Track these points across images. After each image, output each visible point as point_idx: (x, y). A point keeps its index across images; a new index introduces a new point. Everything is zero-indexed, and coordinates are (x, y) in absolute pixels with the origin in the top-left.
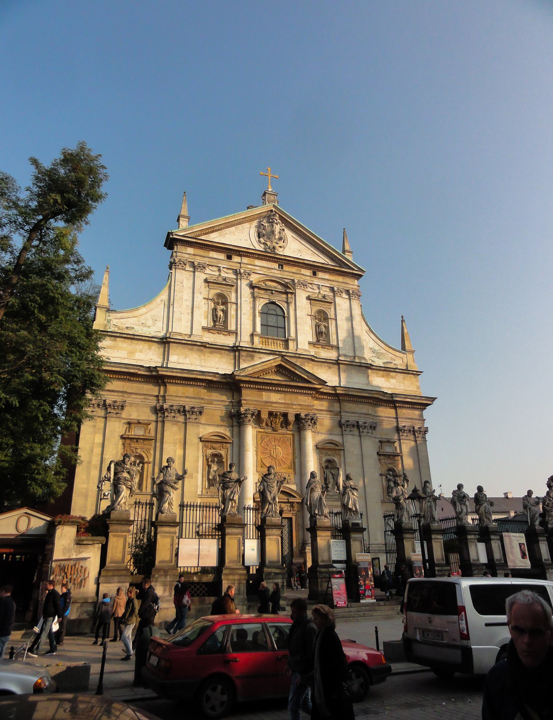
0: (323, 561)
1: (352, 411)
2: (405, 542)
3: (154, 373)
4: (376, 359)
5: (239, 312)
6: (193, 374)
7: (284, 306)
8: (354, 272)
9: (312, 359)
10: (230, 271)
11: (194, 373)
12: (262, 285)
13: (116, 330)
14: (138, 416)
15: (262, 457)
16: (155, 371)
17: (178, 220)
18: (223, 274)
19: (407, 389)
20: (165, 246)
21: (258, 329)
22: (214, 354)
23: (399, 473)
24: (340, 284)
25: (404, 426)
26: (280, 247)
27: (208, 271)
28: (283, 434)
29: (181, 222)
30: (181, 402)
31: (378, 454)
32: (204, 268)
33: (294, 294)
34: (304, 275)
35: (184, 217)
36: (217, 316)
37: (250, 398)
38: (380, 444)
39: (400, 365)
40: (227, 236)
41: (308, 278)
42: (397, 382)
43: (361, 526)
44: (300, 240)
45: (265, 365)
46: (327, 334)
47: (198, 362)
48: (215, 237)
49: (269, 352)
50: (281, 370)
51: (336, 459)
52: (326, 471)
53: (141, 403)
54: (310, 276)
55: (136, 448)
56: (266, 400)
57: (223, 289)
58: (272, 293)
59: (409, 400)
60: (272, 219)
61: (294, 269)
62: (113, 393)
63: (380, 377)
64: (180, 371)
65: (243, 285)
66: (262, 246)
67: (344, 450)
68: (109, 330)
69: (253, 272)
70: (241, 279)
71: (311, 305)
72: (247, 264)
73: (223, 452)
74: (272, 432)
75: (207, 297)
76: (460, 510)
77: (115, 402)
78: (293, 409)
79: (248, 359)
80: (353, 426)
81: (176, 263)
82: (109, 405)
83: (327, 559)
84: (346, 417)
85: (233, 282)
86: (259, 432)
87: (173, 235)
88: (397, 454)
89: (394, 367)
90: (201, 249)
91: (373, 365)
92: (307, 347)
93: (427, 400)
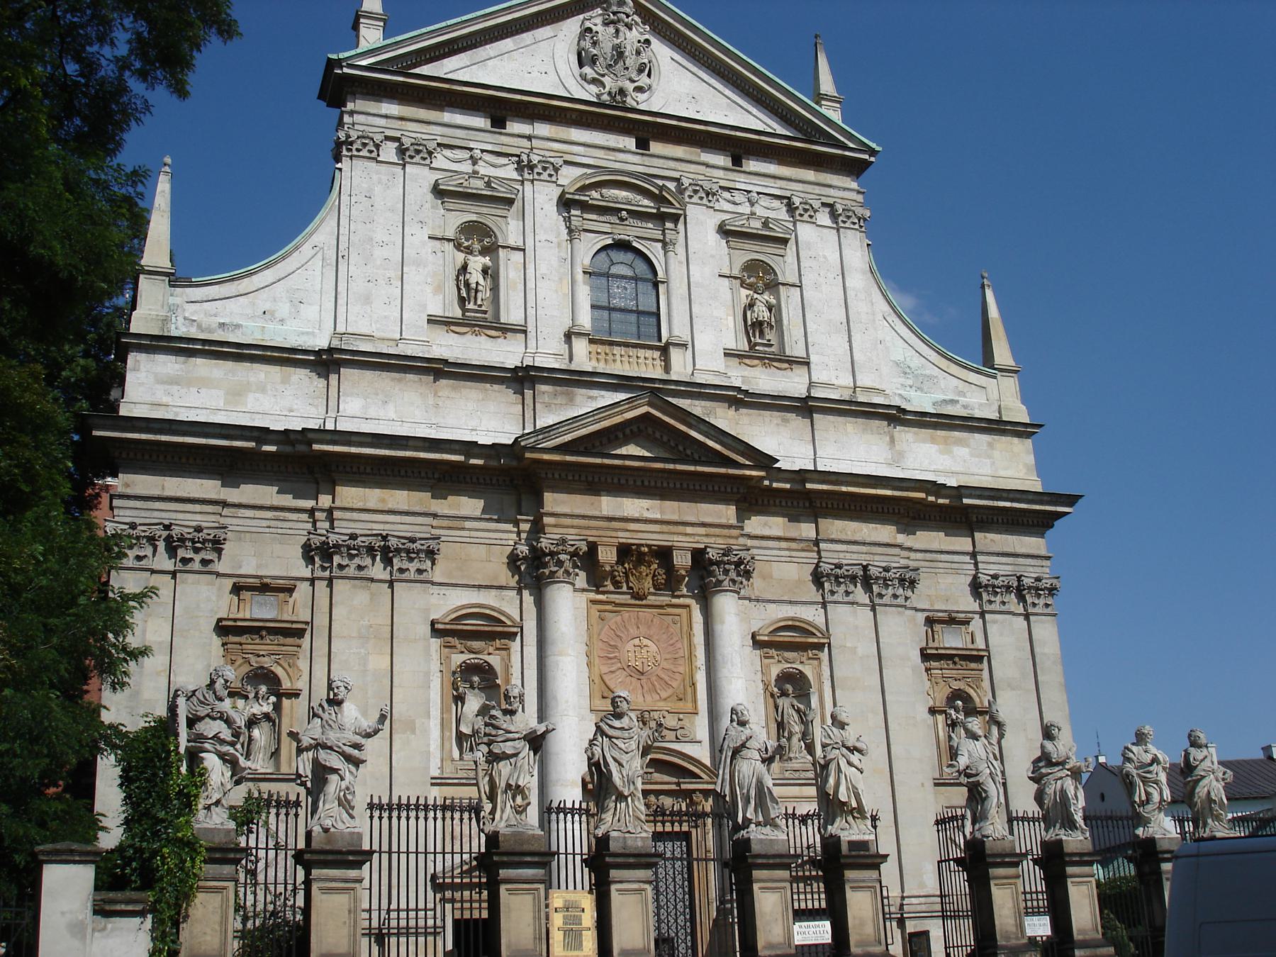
0: (770, 946)
1: (850, 538)
2: (994, 889)
3: (301, 448)
4: (912, 394)
6: (406, 448)
7: (655, 251)
8: (847, 153)
9: (740, 399)
11: (411, 443)
13: (193, 332)
14: (259, 566)
15: (605, 669)
16: (301, 442)
17: (356, 27)
18: (483, 169)
19: (1002, 473)
20: (320, 97)
21: (585, 320)
22: (465, 392)
23: (981, 702)
24: (809, 188)
25: (995, 577)
26: (639, 89)
27: (440, 161)
28: (661, 607)
29: (363, 31)
30: (375, 526)
31: (925, 656)
34: (707, 165)
35: (371, 16)
36: (467, 285)
39: (981, 405)
40: (490, 63)
41: (721, 173)
42: (972, 455)
43: (873, 850)
44: (695, 69)
47: (419, 415)
48: (456, 68)
50: (650, 430)
52: (780, 702)
54: (725, 169)
55: (259, 656)
56: (611, 514)
57: (485, 210)
58: (622, 219)
60: (614, 13)
61: (679, 151)
62: (189, 507)
63: (924, 441)
64: (369, 440)
66: (594, 89)
67: (829, 644)
68: (174, 333)
69: (566, 162)
70: (532, 181)
73: (495, 660)
74: (633, 602)
76: (1144, 798)
77: (199, 529)
78: (686, 534)
79: (559, 400)
80: (853, 578)
81: (351, 143)
82: (179, 540)
83: (781, 940)
84: (833, 554)
86: (594, 602)
87: (341, 67)
89: (963, 413)
91: (904, 411)
92: (719, 363)
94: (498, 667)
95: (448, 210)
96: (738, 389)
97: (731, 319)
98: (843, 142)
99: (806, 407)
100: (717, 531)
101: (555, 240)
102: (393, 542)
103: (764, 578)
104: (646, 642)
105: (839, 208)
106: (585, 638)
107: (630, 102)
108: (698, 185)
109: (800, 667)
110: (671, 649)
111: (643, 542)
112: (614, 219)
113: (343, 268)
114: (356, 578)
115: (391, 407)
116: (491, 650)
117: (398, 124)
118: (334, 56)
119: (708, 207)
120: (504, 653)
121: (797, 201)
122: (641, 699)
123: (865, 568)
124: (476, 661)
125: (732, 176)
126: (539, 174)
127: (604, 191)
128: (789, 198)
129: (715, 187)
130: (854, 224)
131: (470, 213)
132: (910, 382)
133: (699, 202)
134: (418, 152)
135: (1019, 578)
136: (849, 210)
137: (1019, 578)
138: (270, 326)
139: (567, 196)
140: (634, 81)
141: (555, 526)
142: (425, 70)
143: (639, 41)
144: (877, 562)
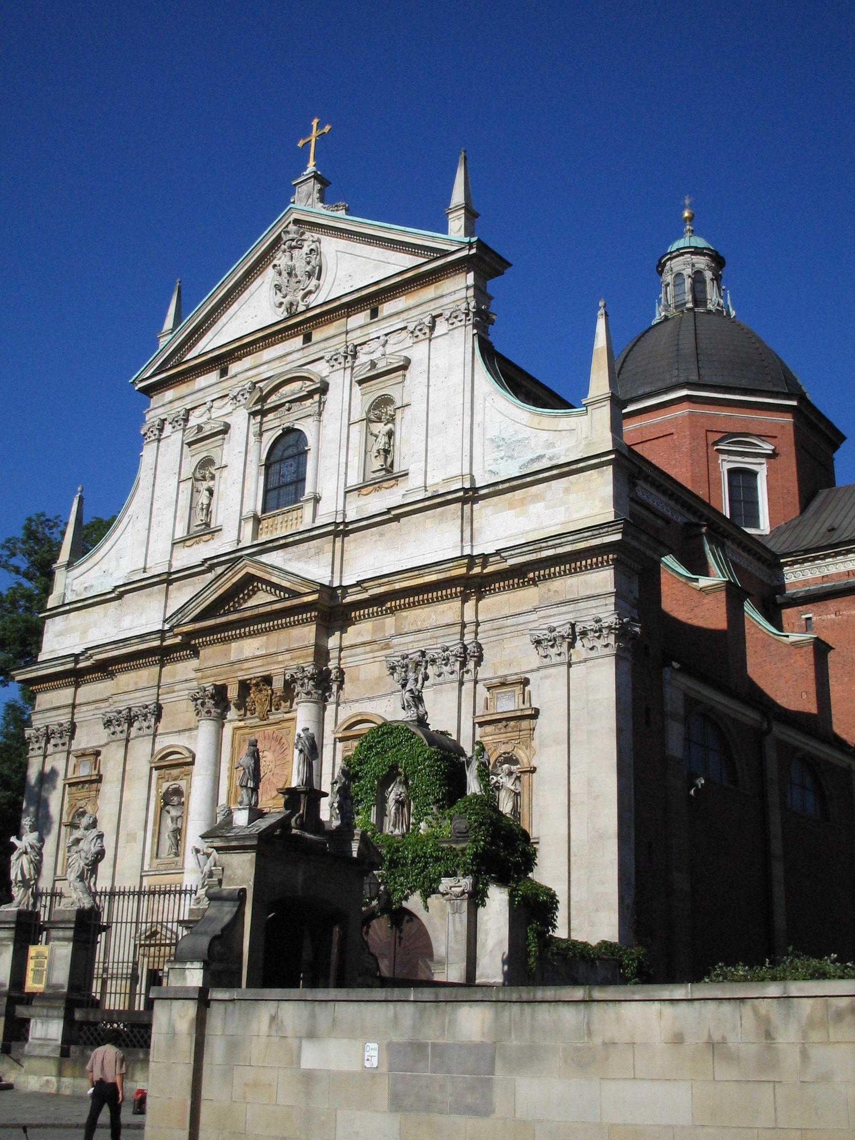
7: (307, 427)
11: (132, 641)
12: (273, 400)
19: (575, 516)
24: (424, 308)
25: (552, 630)
26: (310, 292)
27: (193, 421)
32: (186, 420)
33: (323, 389)
37: (210, 664)
38: (487, 695)
39: (568, 450)
41: (358, 333)
45: (219, 588)
53: (93, 717)
57: (210, 446)
59: (551, 552)
65: (240, 420)
71: (363, 395)
72: (246, 371)
73: (183, 784)
78: (279, 662)
86: (237, 729)
88: (519, 713)
90: (184, 383)
93: (599, 536)
95: (193, 456)
96: (337, 524)
97: (357, 458)
98: (447, 251)
99: (393, 516)
100: (298, 653)
101: (244, 450)
103: (352, 681)
107: (301, 308)
108: (337, 354)
110: (281, 756)
111: (252, 676)
114: (119, 740)
115: (144, 616)
117: (168, 407)
118: (131, 381)
119: (345, 369)
120: (189, 777)
121: (411, 328)
123: (423, 654)
124: (175, 786)
125: (366, 330)
126: (239, 401)
129: (350, 348)
130: (461, 321)
131: (202, 451)
132: (502, 454)
133: (338, 367)
134: (177, 421)
137: (573, 626)
139: (249, 411)
140: (303, 290)
141: (202, 678)
143: (307, 254)
144: (433, 646)
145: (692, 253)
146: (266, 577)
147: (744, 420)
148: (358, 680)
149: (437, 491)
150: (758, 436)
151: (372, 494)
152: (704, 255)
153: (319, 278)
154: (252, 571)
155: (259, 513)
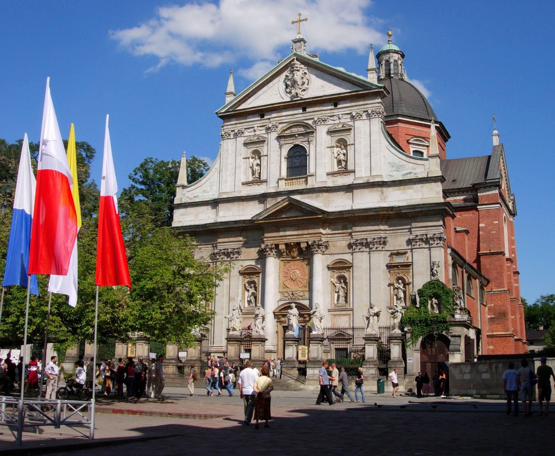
0: (169, 356)
1: (363, 230)
4: (395, 173)
5: (269, 162)
10: (264, 128)
11: (230, 223)
12: (288, 132)
18: (257, 133)
19: (425, 197)
21: (284, 173)
25: (417, 236)
26: (304, 90)
27: (247, 133)
32: (243, 133)
39: (421, 172)
41: (329, 111)
46: (346, 162)
49: (287, 192)
51: (346, 275)
57: (257, 146)
59: (419, 210)
63: (396, 190)
75: (245, 157)
85: (263, 137)
92: (324, 178)
94: (257, 282)
100: (313, 235)
102: (229, 251)
104: (296, 271)
105: (370, 112)
106: (278, 272)
109: (344, 274)
112: (294, 138)
113: (221, 173)
116: (255, 277)
121: (354, 114)
122: (294, 288)
123: (366, 239)
127: (291, 130)
128: (352, 113)
131: (254, 148)
132: (394, 169)
134: (239, 133)
135: (426, 235)
136: (373, 111)
138: (205, 194)
142: (243, 107)
145: (393, 52)
146: (300, 205)
147: (419, 130)
148: (337, 246)
149: (369, 180)
150: (424, 138)
151: (339, 177)
152: (398, 53)
153: (308, 85)
154: (292, 202)
155: (285, 177)
